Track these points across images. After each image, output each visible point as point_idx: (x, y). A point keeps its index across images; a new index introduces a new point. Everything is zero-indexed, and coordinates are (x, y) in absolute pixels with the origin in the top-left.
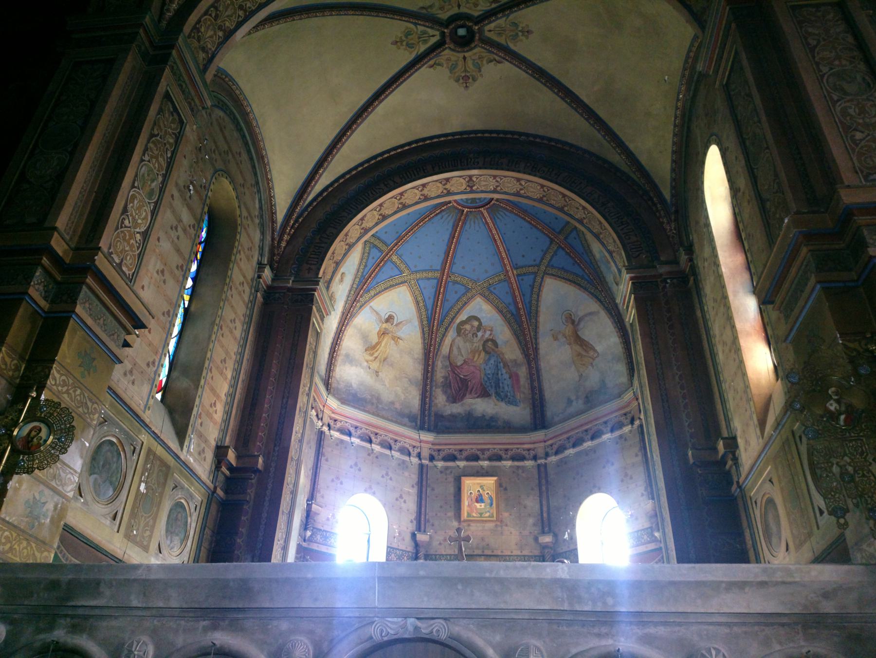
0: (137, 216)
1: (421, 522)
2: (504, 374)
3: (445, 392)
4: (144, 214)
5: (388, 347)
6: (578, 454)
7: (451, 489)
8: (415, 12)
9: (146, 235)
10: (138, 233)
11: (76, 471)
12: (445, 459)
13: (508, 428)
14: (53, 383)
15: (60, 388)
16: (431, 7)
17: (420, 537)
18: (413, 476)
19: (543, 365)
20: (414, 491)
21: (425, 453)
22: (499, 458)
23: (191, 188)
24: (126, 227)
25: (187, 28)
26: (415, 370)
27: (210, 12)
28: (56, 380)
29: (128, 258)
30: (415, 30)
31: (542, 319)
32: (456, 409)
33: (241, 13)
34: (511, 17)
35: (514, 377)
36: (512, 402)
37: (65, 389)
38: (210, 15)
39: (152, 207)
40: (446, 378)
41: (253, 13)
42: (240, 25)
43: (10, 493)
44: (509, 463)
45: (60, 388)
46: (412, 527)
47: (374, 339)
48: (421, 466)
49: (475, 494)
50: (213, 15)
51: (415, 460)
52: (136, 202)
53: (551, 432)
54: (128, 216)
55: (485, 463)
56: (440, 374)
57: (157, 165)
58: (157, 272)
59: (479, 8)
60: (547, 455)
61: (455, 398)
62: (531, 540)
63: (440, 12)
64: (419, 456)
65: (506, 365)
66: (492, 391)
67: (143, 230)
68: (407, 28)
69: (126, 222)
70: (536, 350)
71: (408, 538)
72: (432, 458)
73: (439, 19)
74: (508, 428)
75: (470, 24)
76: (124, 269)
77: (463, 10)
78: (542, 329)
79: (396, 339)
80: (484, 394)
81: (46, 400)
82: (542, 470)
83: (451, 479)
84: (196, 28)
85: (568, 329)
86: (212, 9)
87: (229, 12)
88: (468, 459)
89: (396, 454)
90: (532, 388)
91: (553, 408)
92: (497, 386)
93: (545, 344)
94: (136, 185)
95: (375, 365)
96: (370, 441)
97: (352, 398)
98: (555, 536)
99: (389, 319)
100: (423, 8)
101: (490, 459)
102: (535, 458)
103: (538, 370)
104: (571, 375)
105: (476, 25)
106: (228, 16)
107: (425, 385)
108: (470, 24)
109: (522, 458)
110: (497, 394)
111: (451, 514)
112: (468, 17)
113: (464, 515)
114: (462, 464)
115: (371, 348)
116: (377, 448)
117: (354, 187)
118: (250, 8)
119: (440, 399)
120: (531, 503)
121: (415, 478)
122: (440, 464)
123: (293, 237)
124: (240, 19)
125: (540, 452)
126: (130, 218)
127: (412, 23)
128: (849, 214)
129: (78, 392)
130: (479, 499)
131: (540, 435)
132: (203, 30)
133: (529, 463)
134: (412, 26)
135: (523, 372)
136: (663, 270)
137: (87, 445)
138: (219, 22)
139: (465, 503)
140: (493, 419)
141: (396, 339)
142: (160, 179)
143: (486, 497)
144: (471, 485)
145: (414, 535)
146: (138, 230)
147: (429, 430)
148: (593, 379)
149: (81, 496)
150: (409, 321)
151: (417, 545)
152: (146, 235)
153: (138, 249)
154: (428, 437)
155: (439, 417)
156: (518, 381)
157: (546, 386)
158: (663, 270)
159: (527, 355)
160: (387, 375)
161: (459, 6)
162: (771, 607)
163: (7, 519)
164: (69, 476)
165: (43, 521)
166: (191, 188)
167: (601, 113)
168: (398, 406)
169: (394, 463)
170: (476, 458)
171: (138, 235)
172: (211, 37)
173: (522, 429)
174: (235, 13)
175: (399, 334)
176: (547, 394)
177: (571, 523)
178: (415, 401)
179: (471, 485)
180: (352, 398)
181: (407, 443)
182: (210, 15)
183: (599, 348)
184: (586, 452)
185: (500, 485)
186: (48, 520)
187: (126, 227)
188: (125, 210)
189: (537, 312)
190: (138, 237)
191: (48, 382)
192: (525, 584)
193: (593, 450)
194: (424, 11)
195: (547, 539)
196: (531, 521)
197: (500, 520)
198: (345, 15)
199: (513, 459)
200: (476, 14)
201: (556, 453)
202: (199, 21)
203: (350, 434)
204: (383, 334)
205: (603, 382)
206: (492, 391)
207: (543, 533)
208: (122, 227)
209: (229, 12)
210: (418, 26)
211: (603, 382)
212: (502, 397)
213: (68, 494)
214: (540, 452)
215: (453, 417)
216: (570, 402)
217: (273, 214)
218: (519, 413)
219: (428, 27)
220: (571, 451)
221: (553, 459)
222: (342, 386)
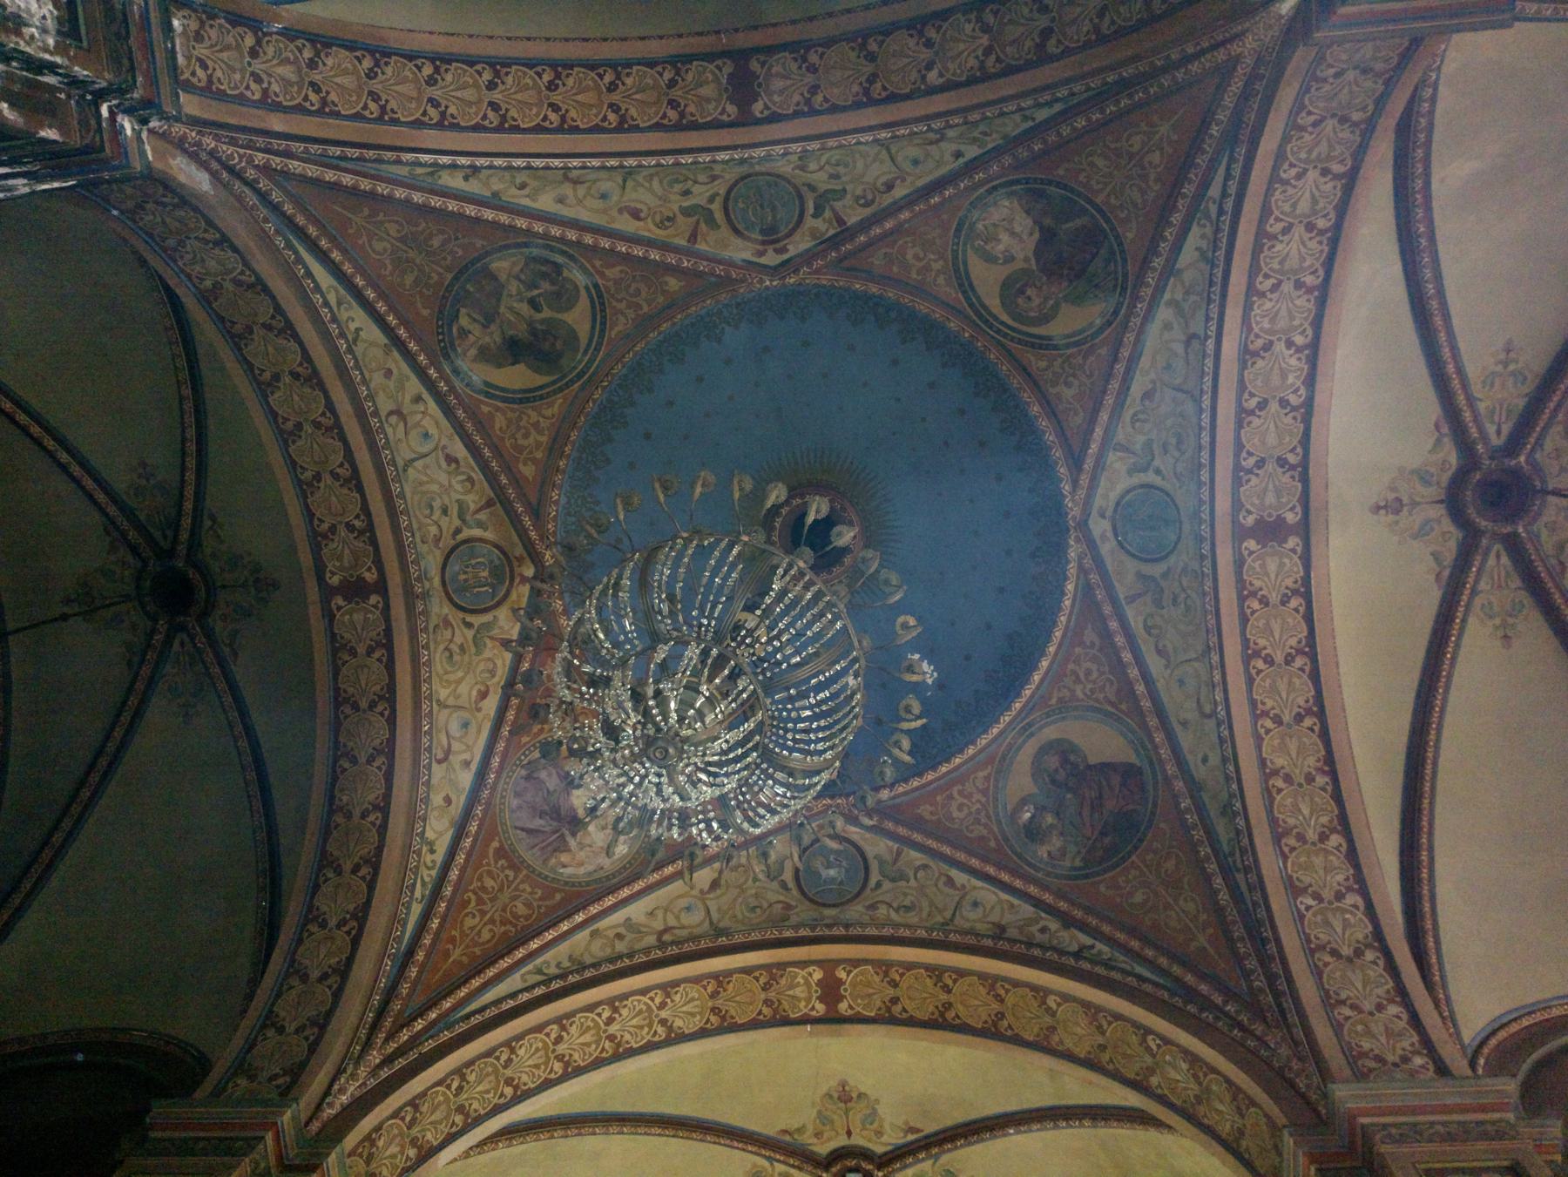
8: (773, 1138)
16: (800, 1130)
25: (351, 1140)
27: (403, 1114)
30: (770, 1169)
33: (459, 1119)
34: (945, 1158)
38: (403, 1119)
41: (479, 1120)
42: (451, 1138)
50: (408, 1119)
59: (885, 1139)
63: (815, 1141)
68: (755, 1165)
73: (813, 1153)
75: (870, 1167)
77: (858, 1140)
84: (369, 1139)
86: (408, 1108)
87: (437, 1116)
100: (785, 1132)
105: (879, 1170)
106: (431, 1123)
108: (870, 1167)
112: (865, 1154)
118: (476, 1111)
124: (454, 1129)
127: (765, 1157)
132: (381, 1143)
134: (766, 1163)
138: (415, 1131)
161: (849, 1133)
172: (393, 1156)
174: (447, 1117)
182: (403, 1119)
194: (787, 1138)
198: (645, 1134)
200: (879, 1149)
202: (378, 1128)
209: (437, 1116)
210: (776, 1164)
219: (793, 1166)
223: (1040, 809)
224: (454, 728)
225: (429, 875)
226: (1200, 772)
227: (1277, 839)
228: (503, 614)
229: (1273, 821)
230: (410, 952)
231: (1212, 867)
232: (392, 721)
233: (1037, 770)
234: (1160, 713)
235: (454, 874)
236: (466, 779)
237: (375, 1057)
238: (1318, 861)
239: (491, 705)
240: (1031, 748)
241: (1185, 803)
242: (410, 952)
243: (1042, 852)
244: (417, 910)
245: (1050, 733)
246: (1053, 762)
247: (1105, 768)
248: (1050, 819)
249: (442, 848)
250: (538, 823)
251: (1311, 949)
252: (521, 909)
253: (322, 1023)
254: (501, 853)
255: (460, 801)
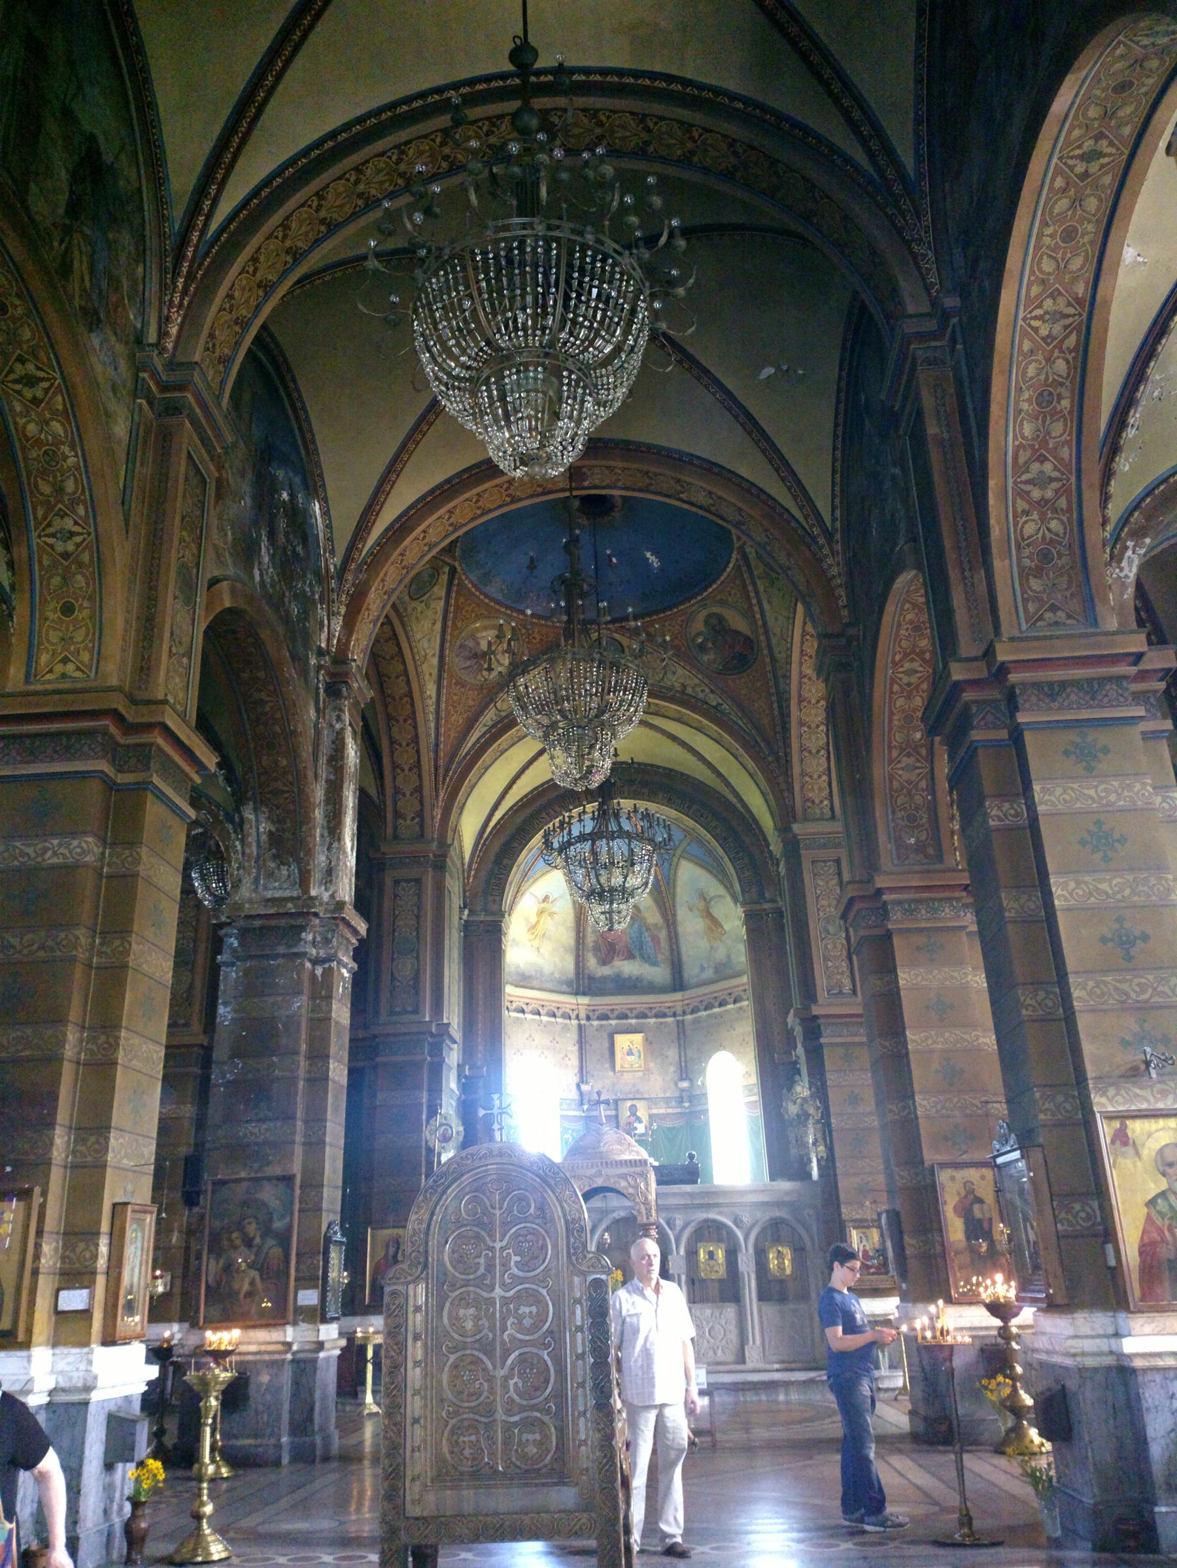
1: (583, 1074)
2: (647, 937)
3: (595, 955)
5: (547, 924)
6: (709, 1016)
7: (606, 1045)
12: (599, 1018)
13: (651, 988)
17: (584, 1088)
18: (573, 1035)
19: (680, 929)
20: (575, 1048)
21: (583, 1015)
22: (645, 1016)
26: (567, 936)
31: (679, 890)
32: (606, 971)
35: (656, 940)
36: (654, 964)
40: (595, 942)
44: (652, 1021)
46: (576, 1079)
47: (534, 919)
48: (580, 1026)
49: (626, 1049)
51: (575, 1022)
53: (688, 994)
55: (633, 1021)
56: (590, 939)
60: (684, 1013)
61: (604, 962)
62: (672, 1085)
64: (577, 1017)
65: (648, 929)
66: (637, 954)
70: (674, 915)
71: (574, 1088)
72: (588, 1018)
74: (651, 988)
78: (679, 899)
79: (551, 914)
80: (630, 956)
82: (681, 1025)
83: (605, 1035)
85: (702, 905)
88: (618, 1018)
89: (559, 1020)
90: (672, 950)
91: (691, 972)
92: (641, 948)
93: (682, 913)
95: (536, 943)
96: (539, 1014)
97: (524, 981)
98: (691, 1080)
99: (546, 899)
101: (637, 1017)
102: (674, 1015)
103: (676, 934)
104: (704, 944)
107: (578, 949)
109: (664, 1015)
110: (642, 957)
111: (607, 1065)
113: (618, 1067)
114: (613, 1022)
115: (532, 928)
116: (545, 1018)
117: (519, 819)
119: (592, 962)
120: (672, 1053)
121: (575, 1037)
122: (595, 1023)
123: (477, 870)
125: (679, 1010)
128: (816, 1017)
130: (630, 1053)
131: (678, 996)
133: (670, 1020)
135: (663, 935)
136: (767, 906)
139: (619, 1055)
140: (639, 979)
141: (551, 914)
143: (635, 1051)
144: (622, 1041)
145: (578, 1086)
147: (584, 994)
148: (720, 954)
150: (561, 897)
151: (581, 1094)
154: (584, 1000)
155: (591, 978)
156: (659, 942)
157: (683, 949)
158: (767, 906)
159: (666, 920)
160: (547, 948)
162: (766, 1199)
167: (722, 770)
168: (557, 975)
169: (558, 1028)
170: (626, 1017)
173: (663, 990)
175: (554, 909)
176: (684, 958)
177: (702, 1072)
178: (568, 965)
179: (622, 1041)
180: (524, 981)
181: (567, 1009)
183: (727, 927)
184: (715, 1016)
185: (646, 1039)
189: (674, 887)
192: (675, 1194)
193: (720, 1015)
195: (685, 1084)
196: (672, 1069)
197: (647, 1071)
199: (656, 1016)
201: (693, 1012)
203: (523, 1011)
204: (541, 912)
205: (729, 956)
206: (637, 954)
207: (682, 1079)
211: (729, 956)
212: (646, 959)
214: (679, 1010)
215: (604, 979)
216: (702, 968)
217: (463, 858)
218: (659, 973)
220: (703, 1013)
221: (689, 1017)
222: (512, 969)
223: (706, 640)
224: (426, 645)
225: (432, 709)
226: (777, 656)
227: (800, 701)
228: (436, 589)
229: (800, 696)
230: (437, 745)
231: (774, 698)
232: (404, 663)
233: (706, 623)
234: (765, 624)
235: (443, 706)
236: (435, 661)
237: (442, 794)
238: (813, 712)
239: (438, 626)
240: (705, 613)
241: (769, 668)
242: (437, 745)
243: (706, 658)
244: (433, 725)
245: (715, 610)
246: (714, 621)
247: (738, 633)
248: (710, 645)
249: (434, 696)
250: (468, 663)
251: (802, 749)
252: (471, 703)
253: (419, 789)
254: (457, 683)
255: (435, 672)
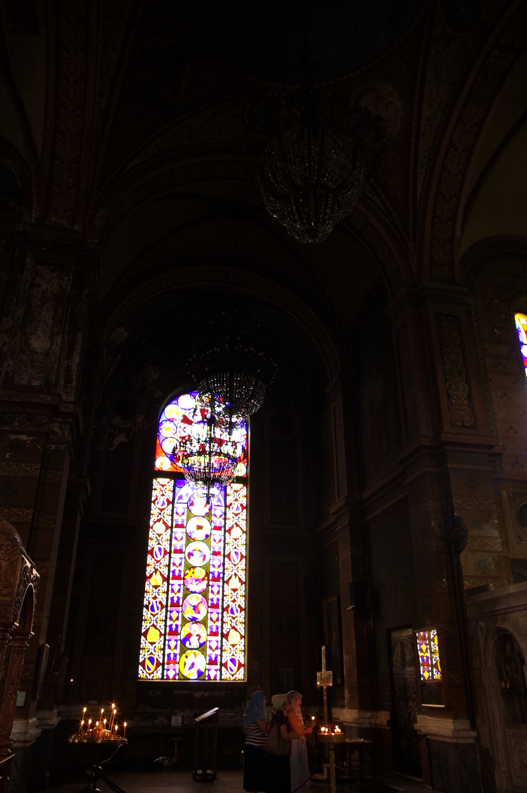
0: (458, 393)
4: (462, 387)
9: (469, 397)
10: (464, 400)
11: (497, 538)
14: (457, 505)
15: (463, 505)
23: (496, 330)
24: (454, 404)
28: (458, 503)
29: (466, 417)
37: (466, 504)
39: (465, 379)
43: (463, 564)
45: (463, 505)
52: (453, 387)
54: (453, 398)
57: (454, 356)
58: (501, 398)
67: (466, 396)
69: (454, 401)
76: (466, 424)
81: (458, 516)
94: (448, 378)
126: (455, 397)
129: (475, 500)
137: (496, 522)
142: (461, 360)
146: (463, 398)
149: (523, 541)
152: (469, 397)
153: (469, 407)
163: (468, 575)
164: (493, 541)
165: (490, 568)
166: (496, 330)
171: (465, 401)
186: (493, 566)
187: (454, 404)
188: (449, 396)
190: (465, 402)
191: (454, 506)
208: (452, 406)
213: (499, 550)
